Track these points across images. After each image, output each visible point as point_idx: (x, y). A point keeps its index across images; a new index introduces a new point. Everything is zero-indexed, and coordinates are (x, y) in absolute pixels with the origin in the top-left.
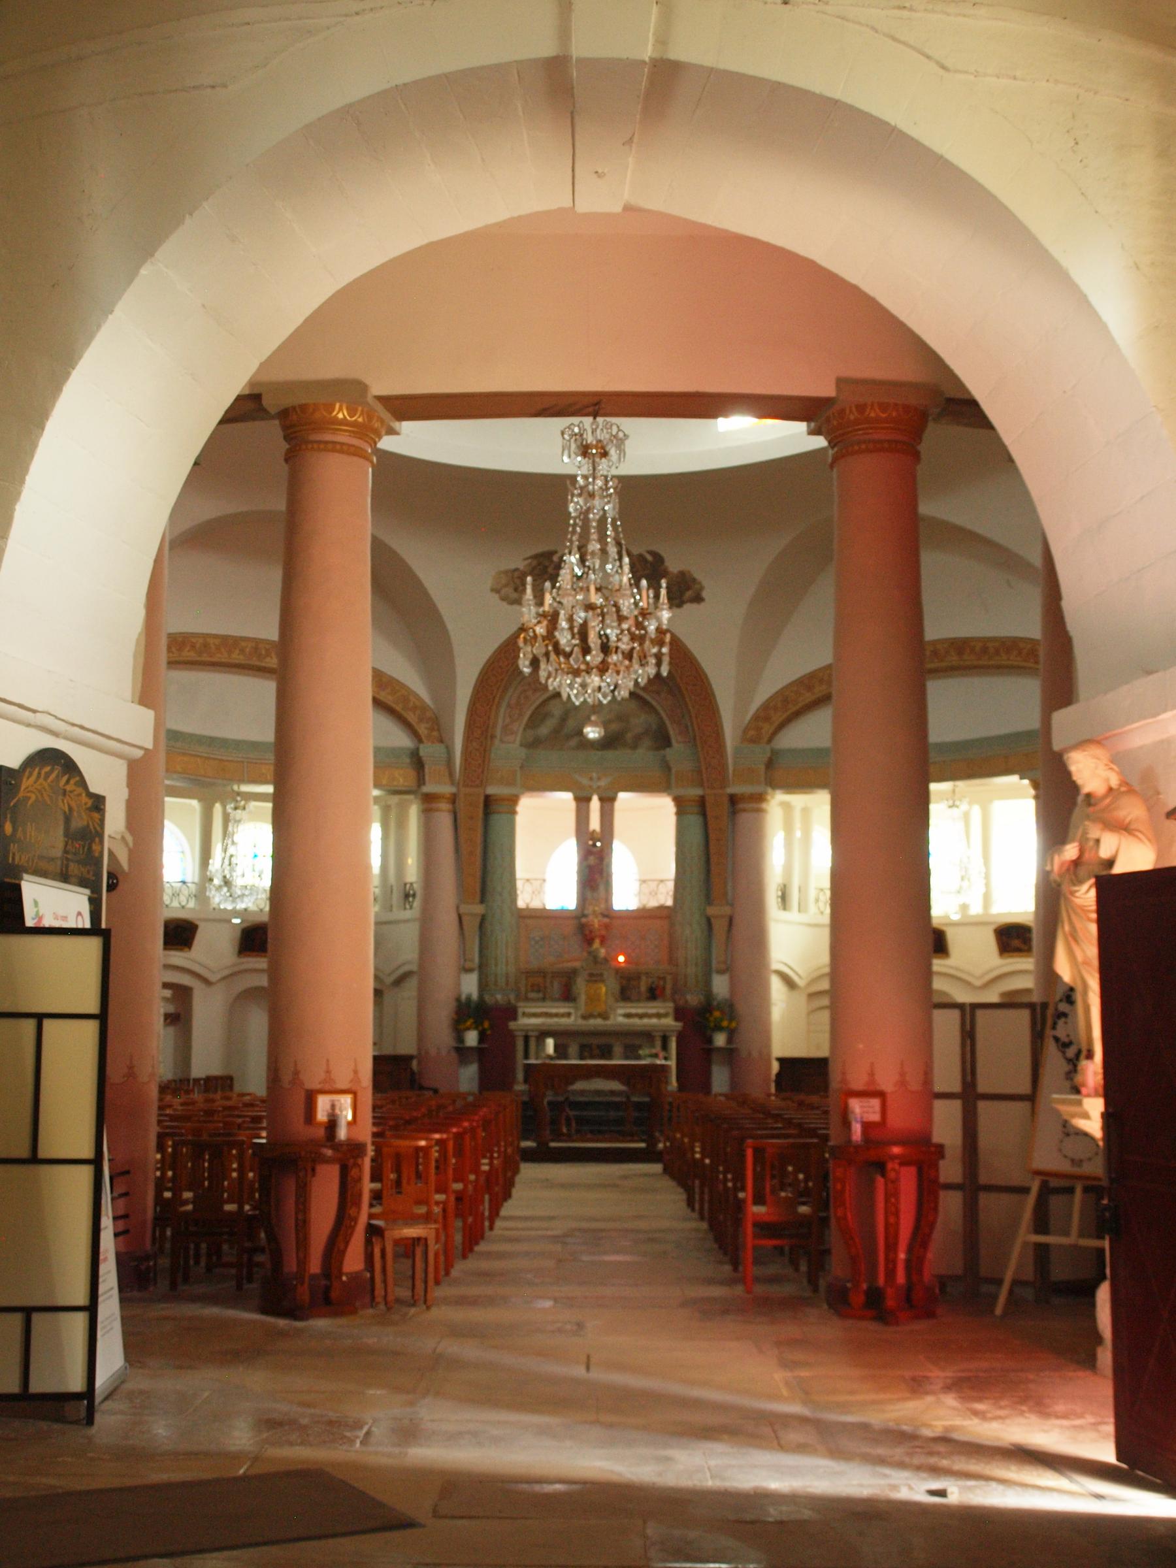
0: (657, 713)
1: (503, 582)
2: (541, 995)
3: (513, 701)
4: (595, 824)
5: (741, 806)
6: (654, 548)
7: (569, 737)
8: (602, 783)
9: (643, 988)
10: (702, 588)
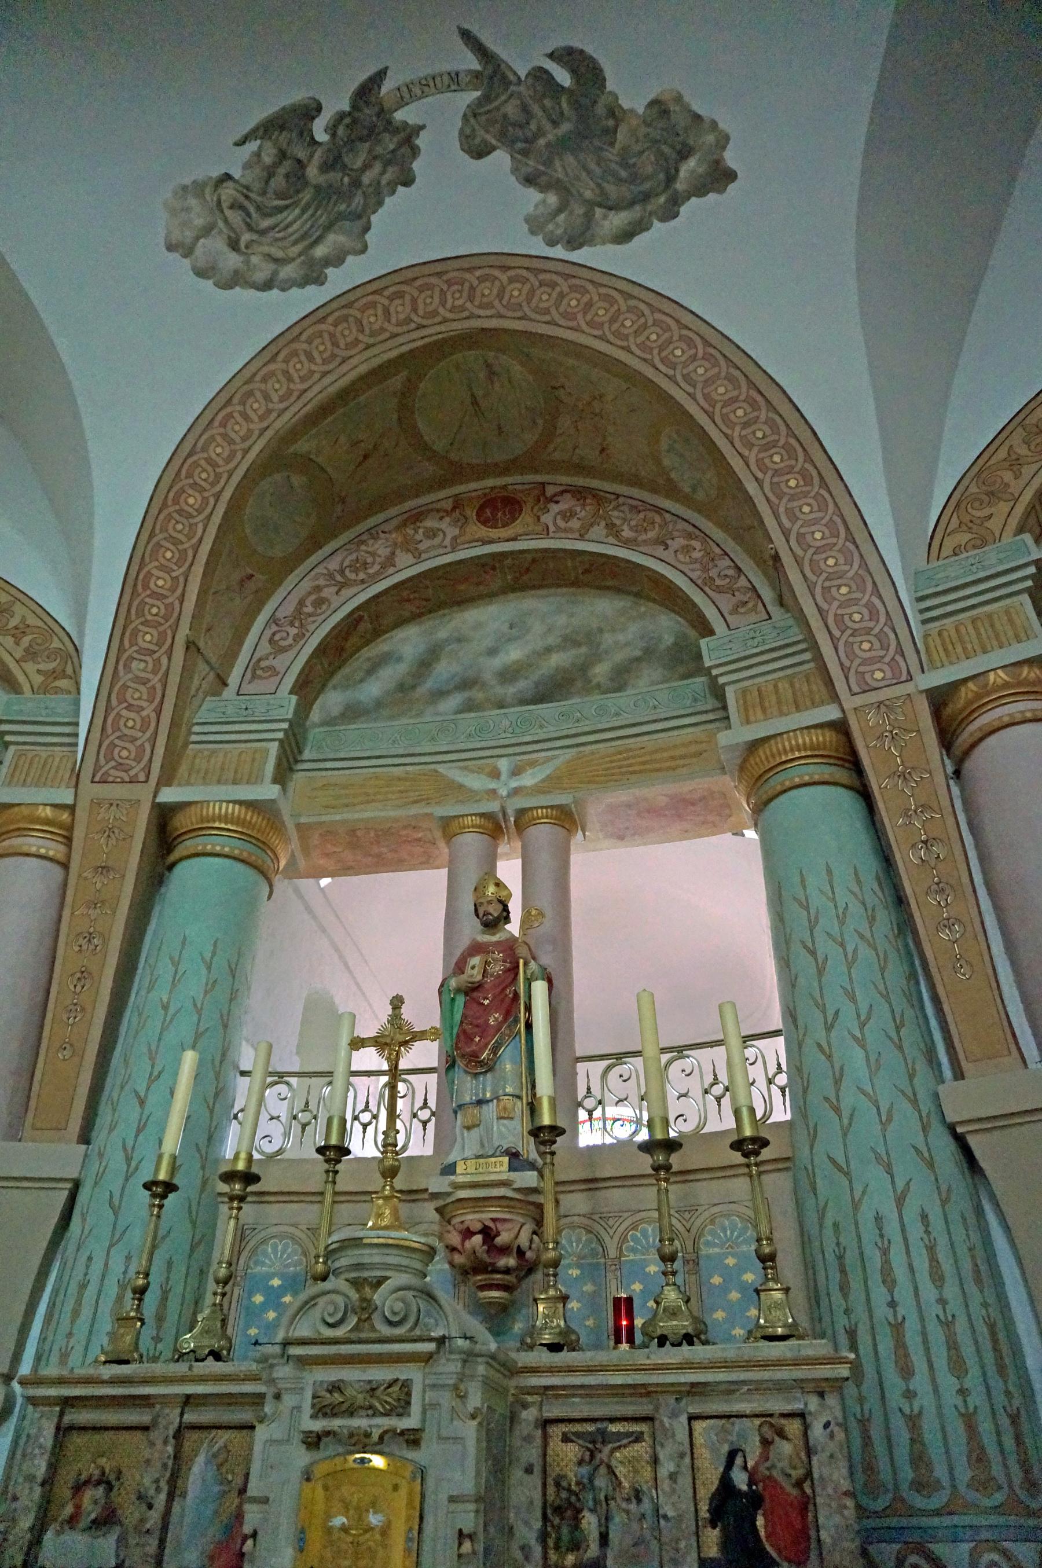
1: (199, 222)
3: (288, 609)
7: (439, 694)
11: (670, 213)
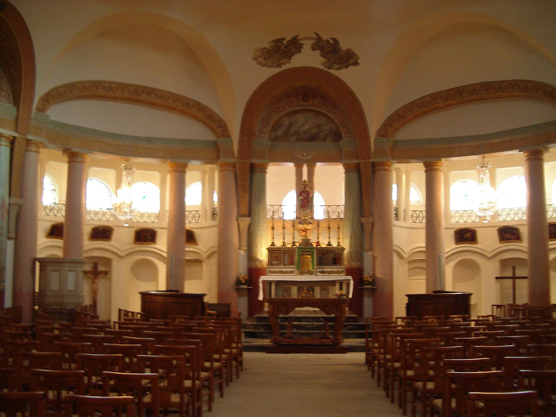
0: (335, 123)
2: (278, 262)
4: (305, 177)
5: (378, 168)
6: (334, 37)
8: (309, 158)
9: (330, 259)
10: (358, 58)
11: (347, 67)
